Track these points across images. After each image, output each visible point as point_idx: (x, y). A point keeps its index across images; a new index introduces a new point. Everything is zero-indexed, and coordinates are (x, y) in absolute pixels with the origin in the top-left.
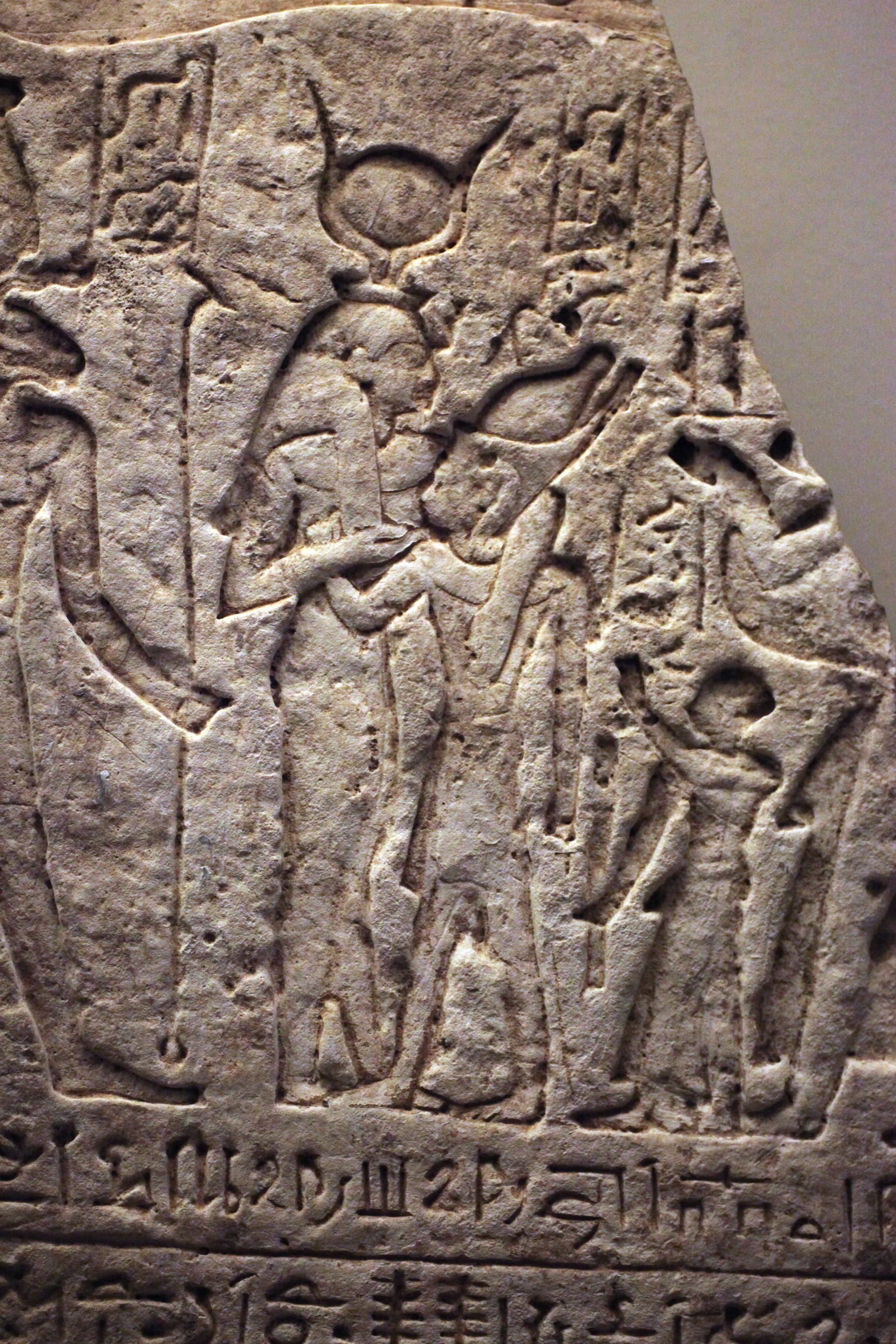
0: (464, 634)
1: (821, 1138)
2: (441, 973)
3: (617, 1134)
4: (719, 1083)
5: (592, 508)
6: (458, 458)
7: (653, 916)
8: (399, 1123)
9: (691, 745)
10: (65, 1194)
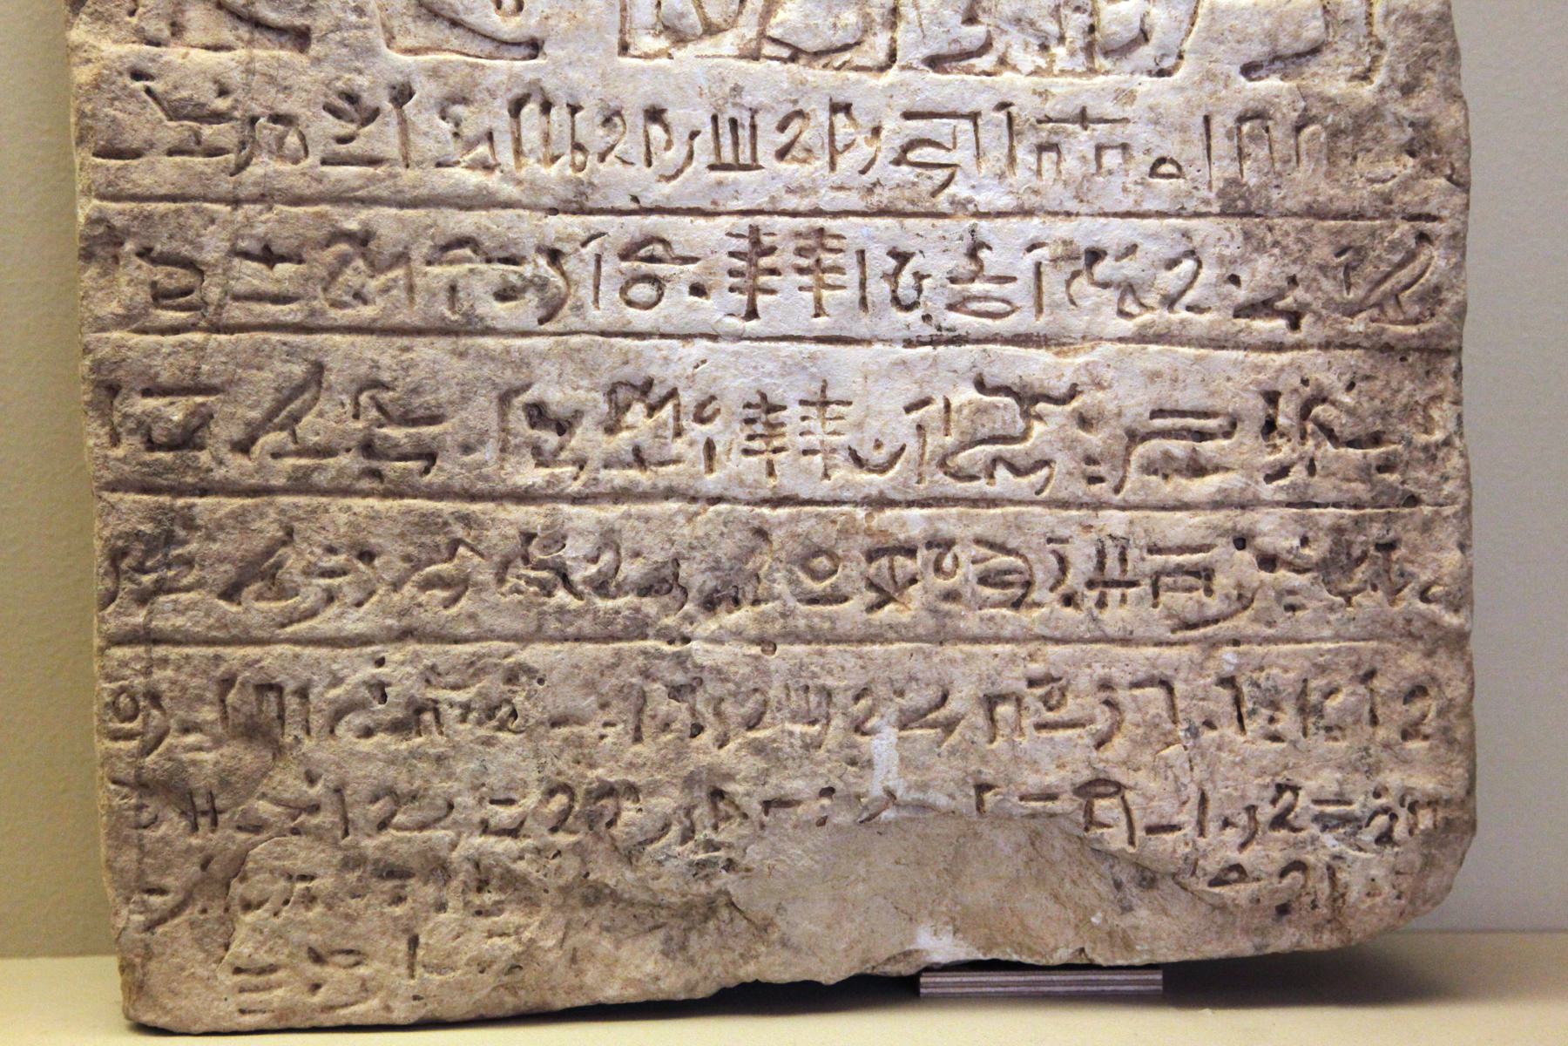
1: (1178, 76)
3: (971, 78)
4: (1072, 24)
8: (747, 74)
10: (406, 157)
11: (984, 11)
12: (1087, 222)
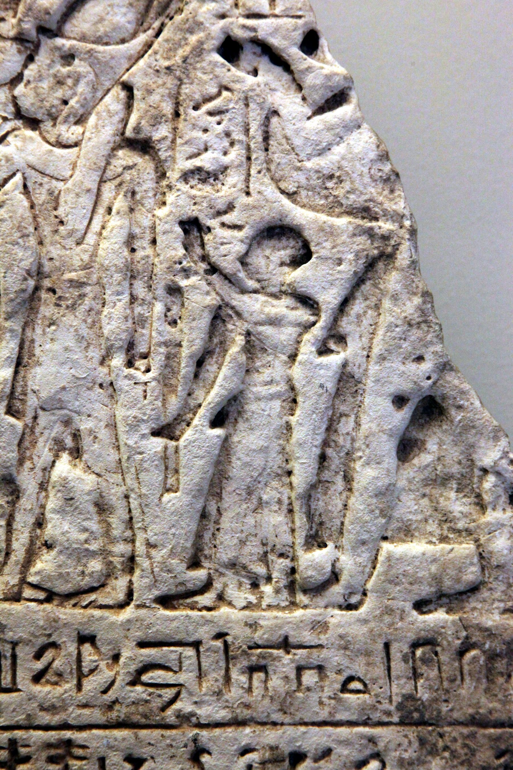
0: (53, 204)
1: (363, 610)
2: (43, 486)
3: (195, 613)
4: (277, 567)
5: (155, 98)
6: (43, 58)
7: (218, 432)
8: (10, 614)
9: (243, 291)
11: (206, 557)
12: (290, 731)
